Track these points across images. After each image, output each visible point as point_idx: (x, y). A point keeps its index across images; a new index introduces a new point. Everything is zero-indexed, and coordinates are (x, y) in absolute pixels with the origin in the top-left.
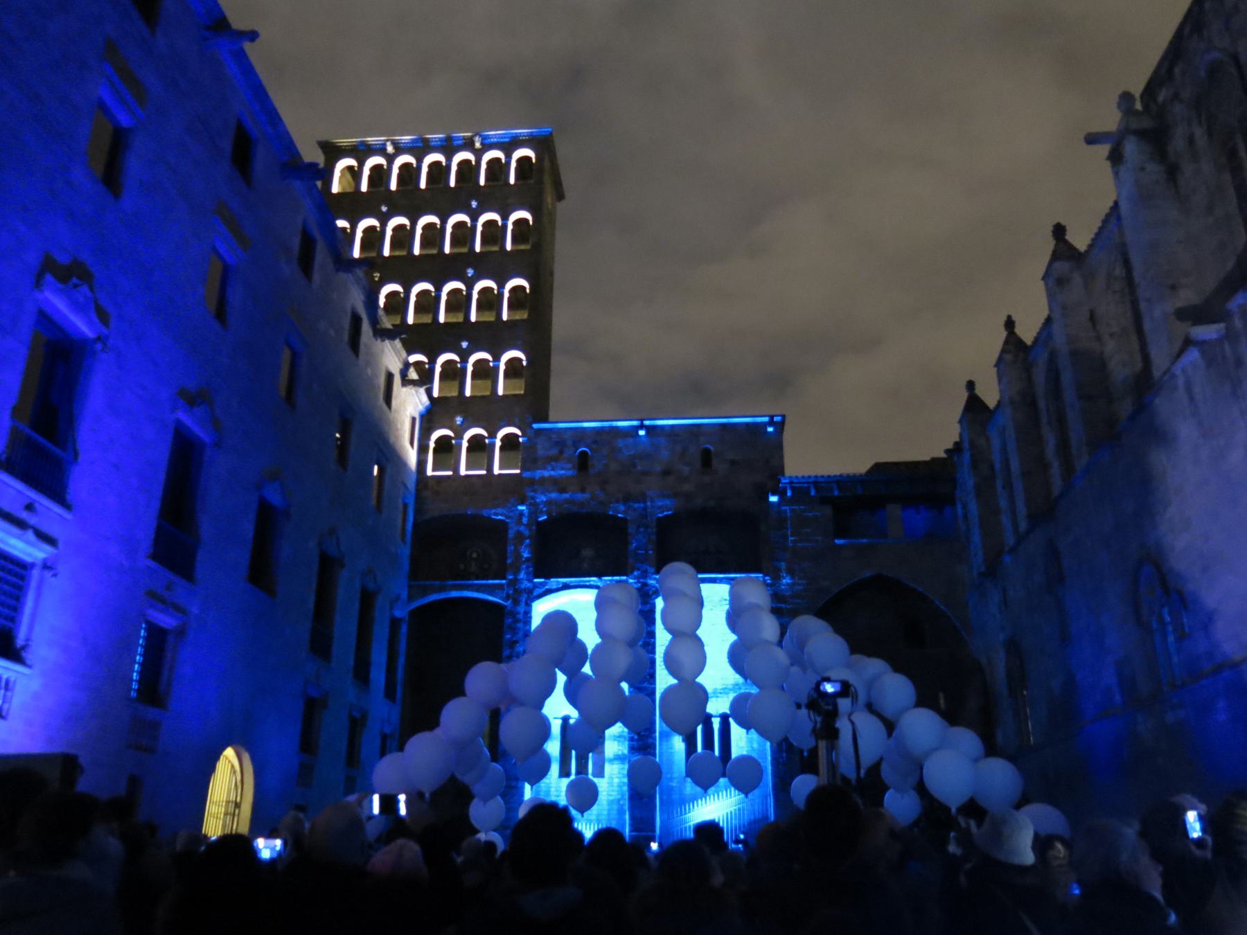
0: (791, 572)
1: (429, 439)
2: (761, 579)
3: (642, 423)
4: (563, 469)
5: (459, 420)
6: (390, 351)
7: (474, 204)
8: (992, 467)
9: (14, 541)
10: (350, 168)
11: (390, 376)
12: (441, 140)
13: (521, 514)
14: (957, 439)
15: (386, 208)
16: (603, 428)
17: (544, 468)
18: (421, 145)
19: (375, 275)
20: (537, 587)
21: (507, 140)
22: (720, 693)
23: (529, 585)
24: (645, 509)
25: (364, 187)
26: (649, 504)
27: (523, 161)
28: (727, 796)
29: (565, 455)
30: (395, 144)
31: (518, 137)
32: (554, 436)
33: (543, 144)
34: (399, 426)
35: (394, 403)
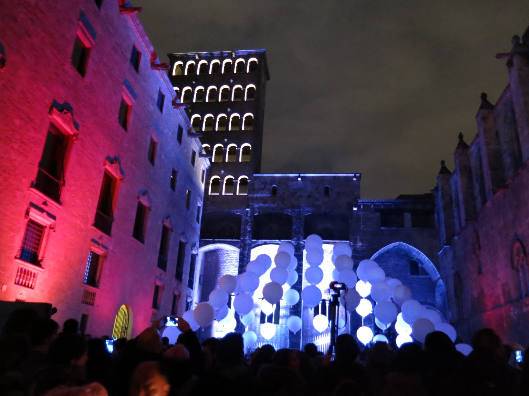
0: (362, 241)
1: (210, 179)
2: (349, 243)
3: (300, 175)
4: (265, 193)
5: (222, 172)
6: (194, 142)
7: (231, 81)
8: (451, 198)
9: (38, 217)
10: (180, 65)
11: (194, 153)
12: (218, 54)
13: (248, 211)
14: (436, 186)
15: (195, 82)
16: (283, 177)
17: (257, 193)
18: (210, 56)
19: (189, 110)
20: (253, 243)
23: (250, 242)
24: (300, 211)
25: (186, 73)
26: (301, 209)
27: (253, 63)
29: (267, 188)
30: (199, 55)
32: (262, 180)
33: (261, 56)
34: (197, 174)
35: (196, 164)
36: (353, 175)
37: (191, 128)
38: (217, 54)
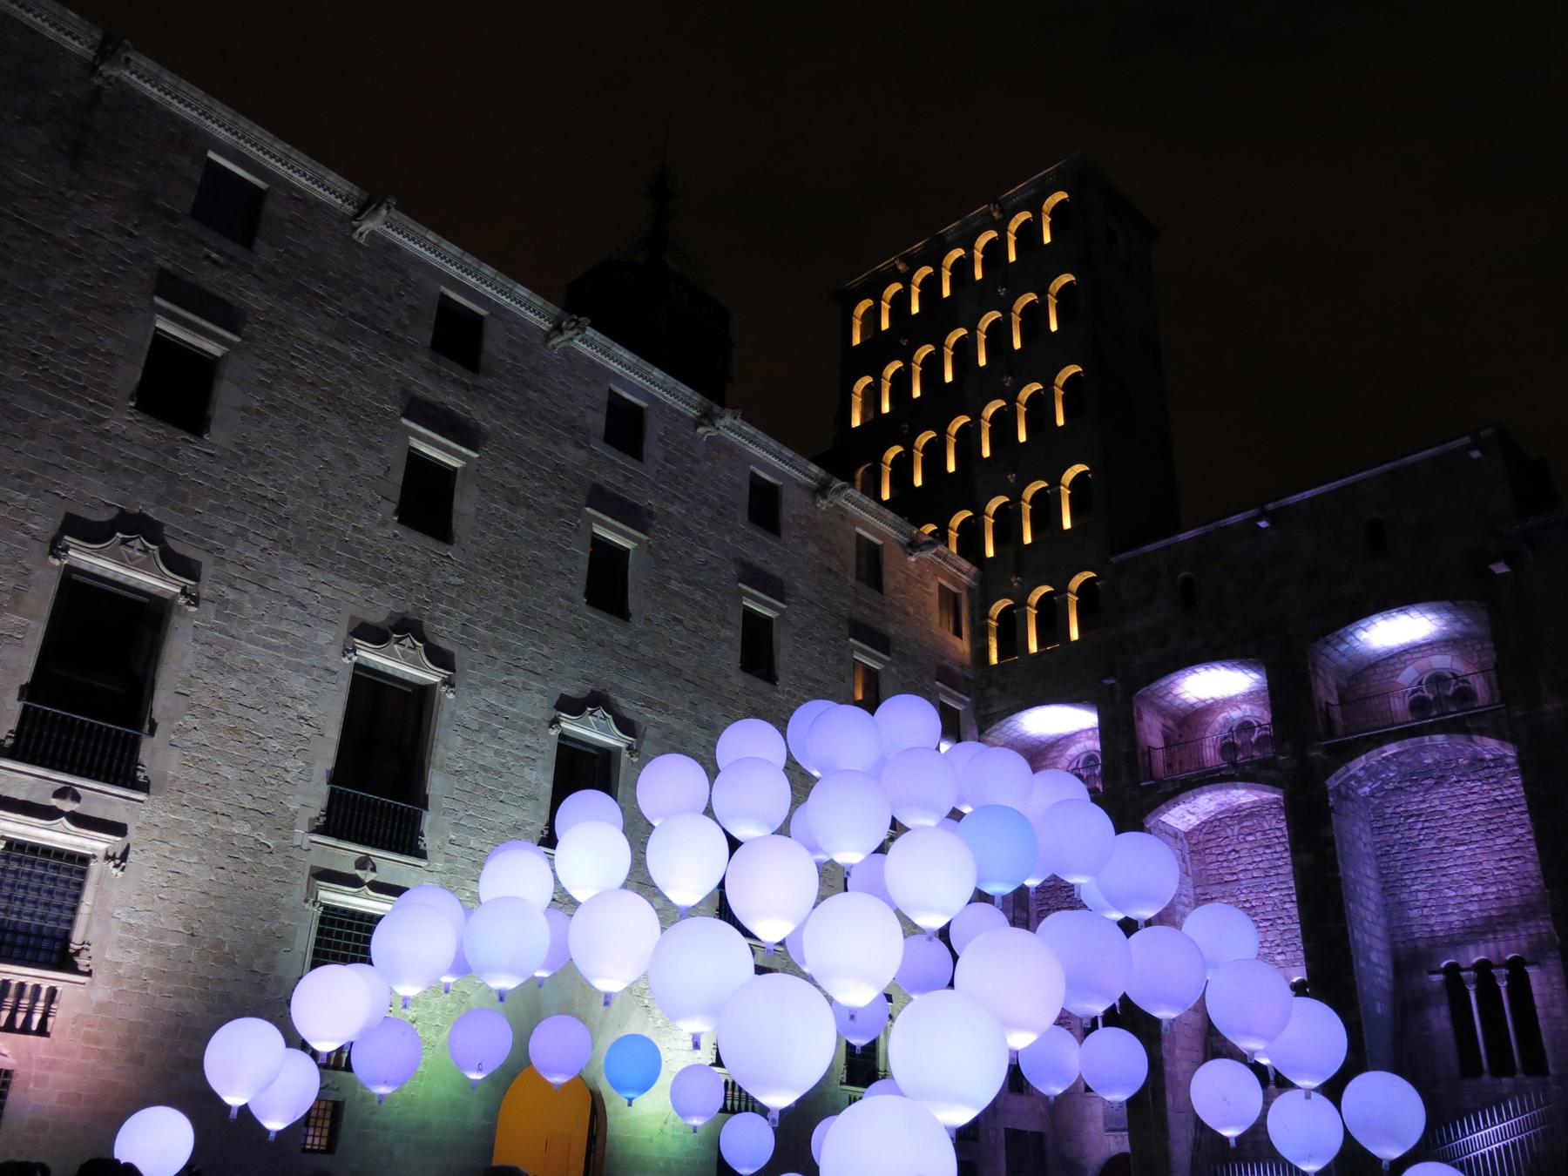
1: (986, 616)
2: (1504, 711)
7: (1002, 291)
9: (45, 833)
12: (957, 229)
22: (1500, 924)
28: (1515, 1110)
30: (903, 259)
34: (911, 610)
35: (889, 582)
36: (1467, 440)
38: (952, 234)
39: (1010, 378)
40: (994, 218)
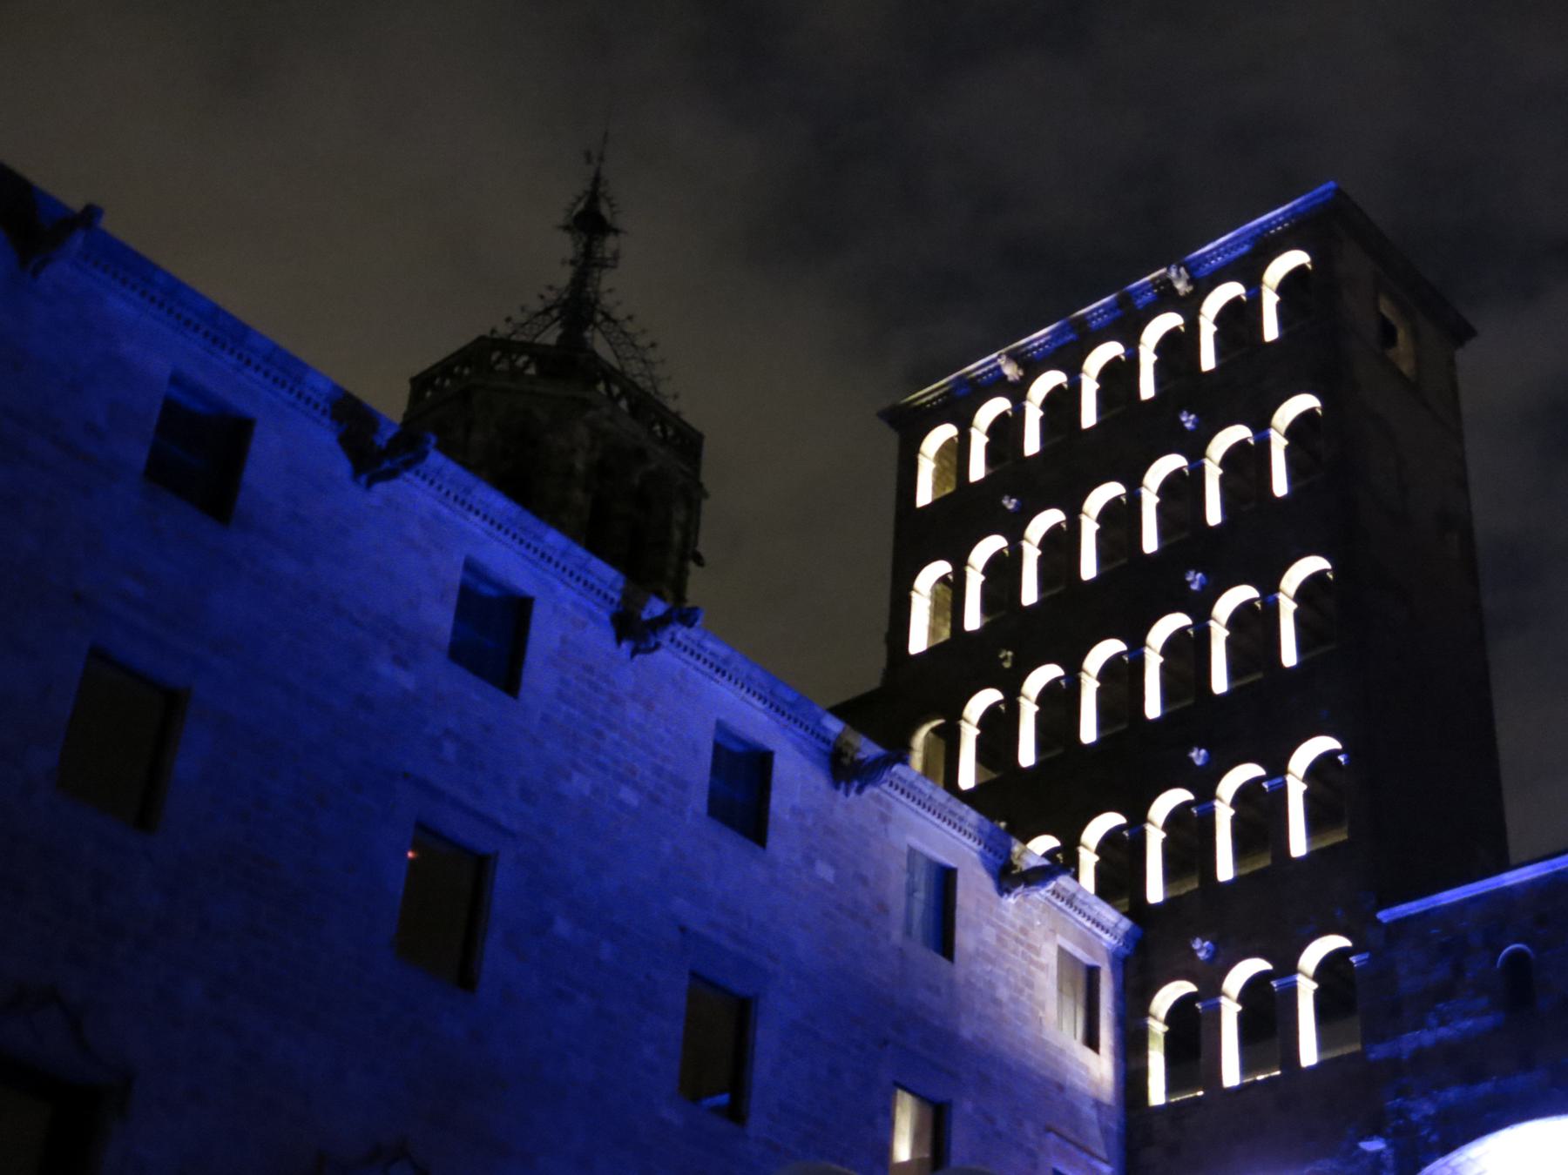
1: (1145, 1012)
5: (1201, 948)
7: (1188, 420)
11: (945, 879)
13: (1379, 1153)
18: (1071, 337)
19: (1002, 656)
21: (1245, 248)
30: (1014, 356)
31: (1267, 231)
34: (1003, 993)
35: (965, 939)
37: (839, 737)
39: (1199, 575)
40: (1175, 291)
